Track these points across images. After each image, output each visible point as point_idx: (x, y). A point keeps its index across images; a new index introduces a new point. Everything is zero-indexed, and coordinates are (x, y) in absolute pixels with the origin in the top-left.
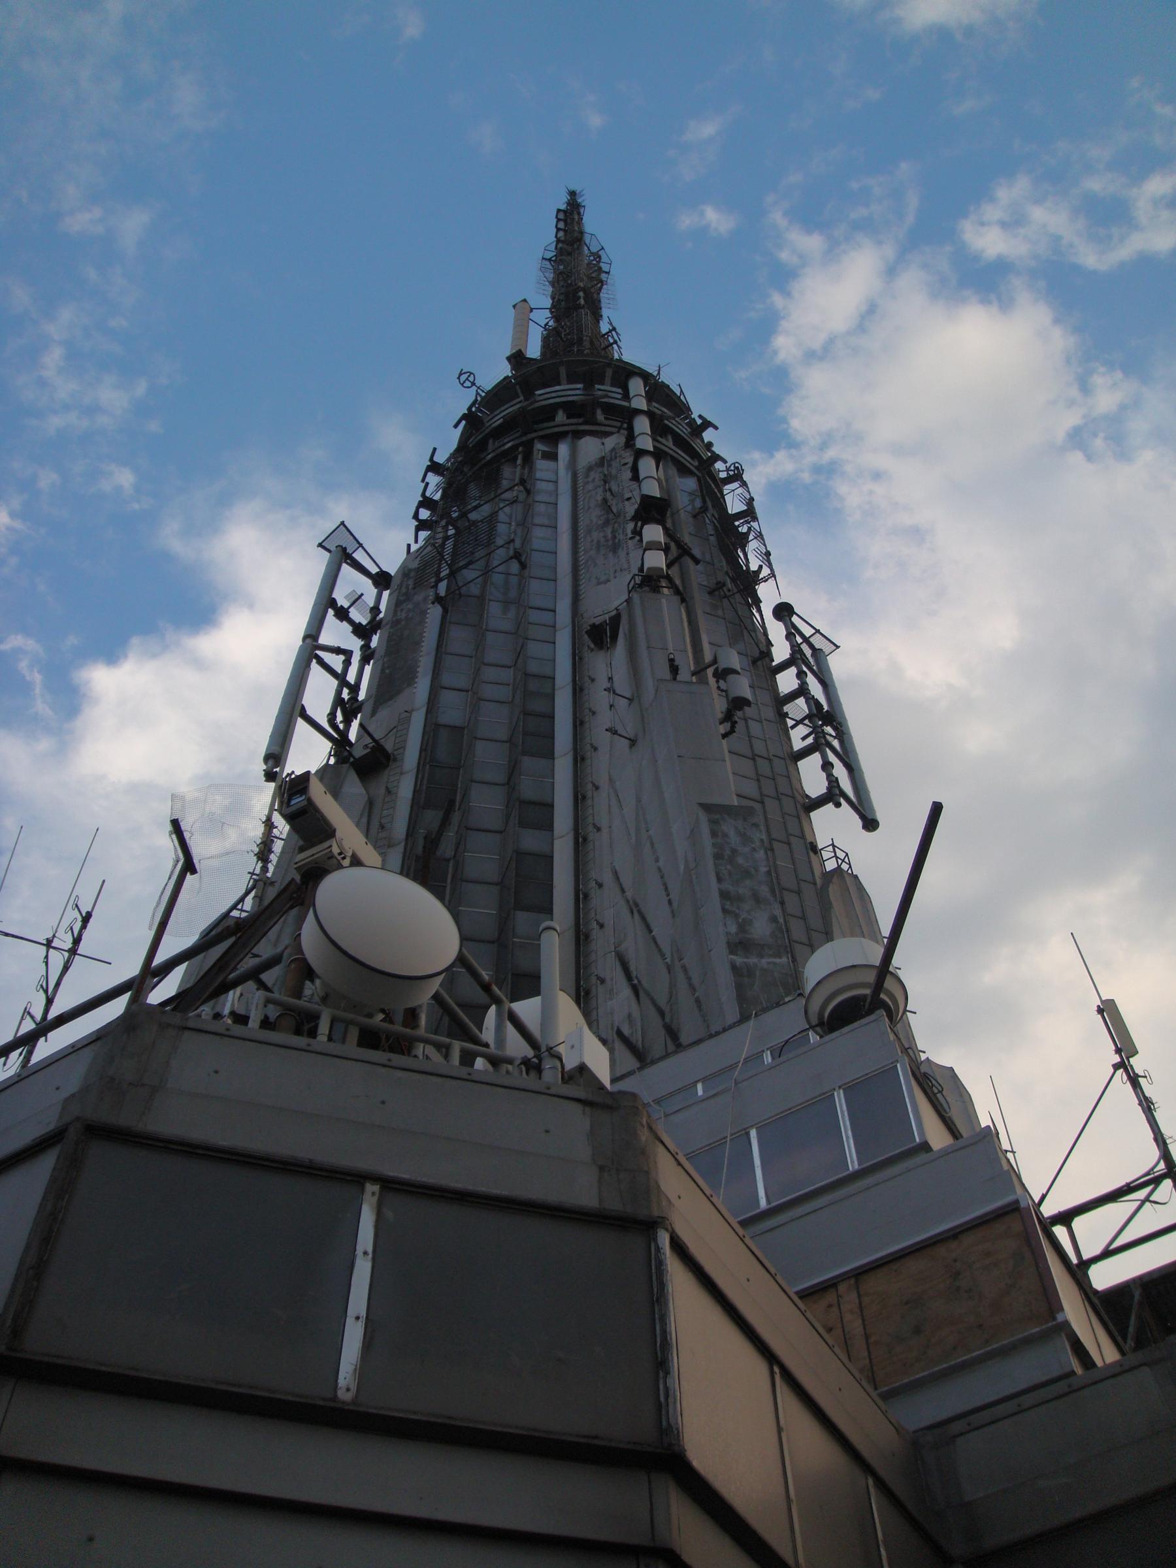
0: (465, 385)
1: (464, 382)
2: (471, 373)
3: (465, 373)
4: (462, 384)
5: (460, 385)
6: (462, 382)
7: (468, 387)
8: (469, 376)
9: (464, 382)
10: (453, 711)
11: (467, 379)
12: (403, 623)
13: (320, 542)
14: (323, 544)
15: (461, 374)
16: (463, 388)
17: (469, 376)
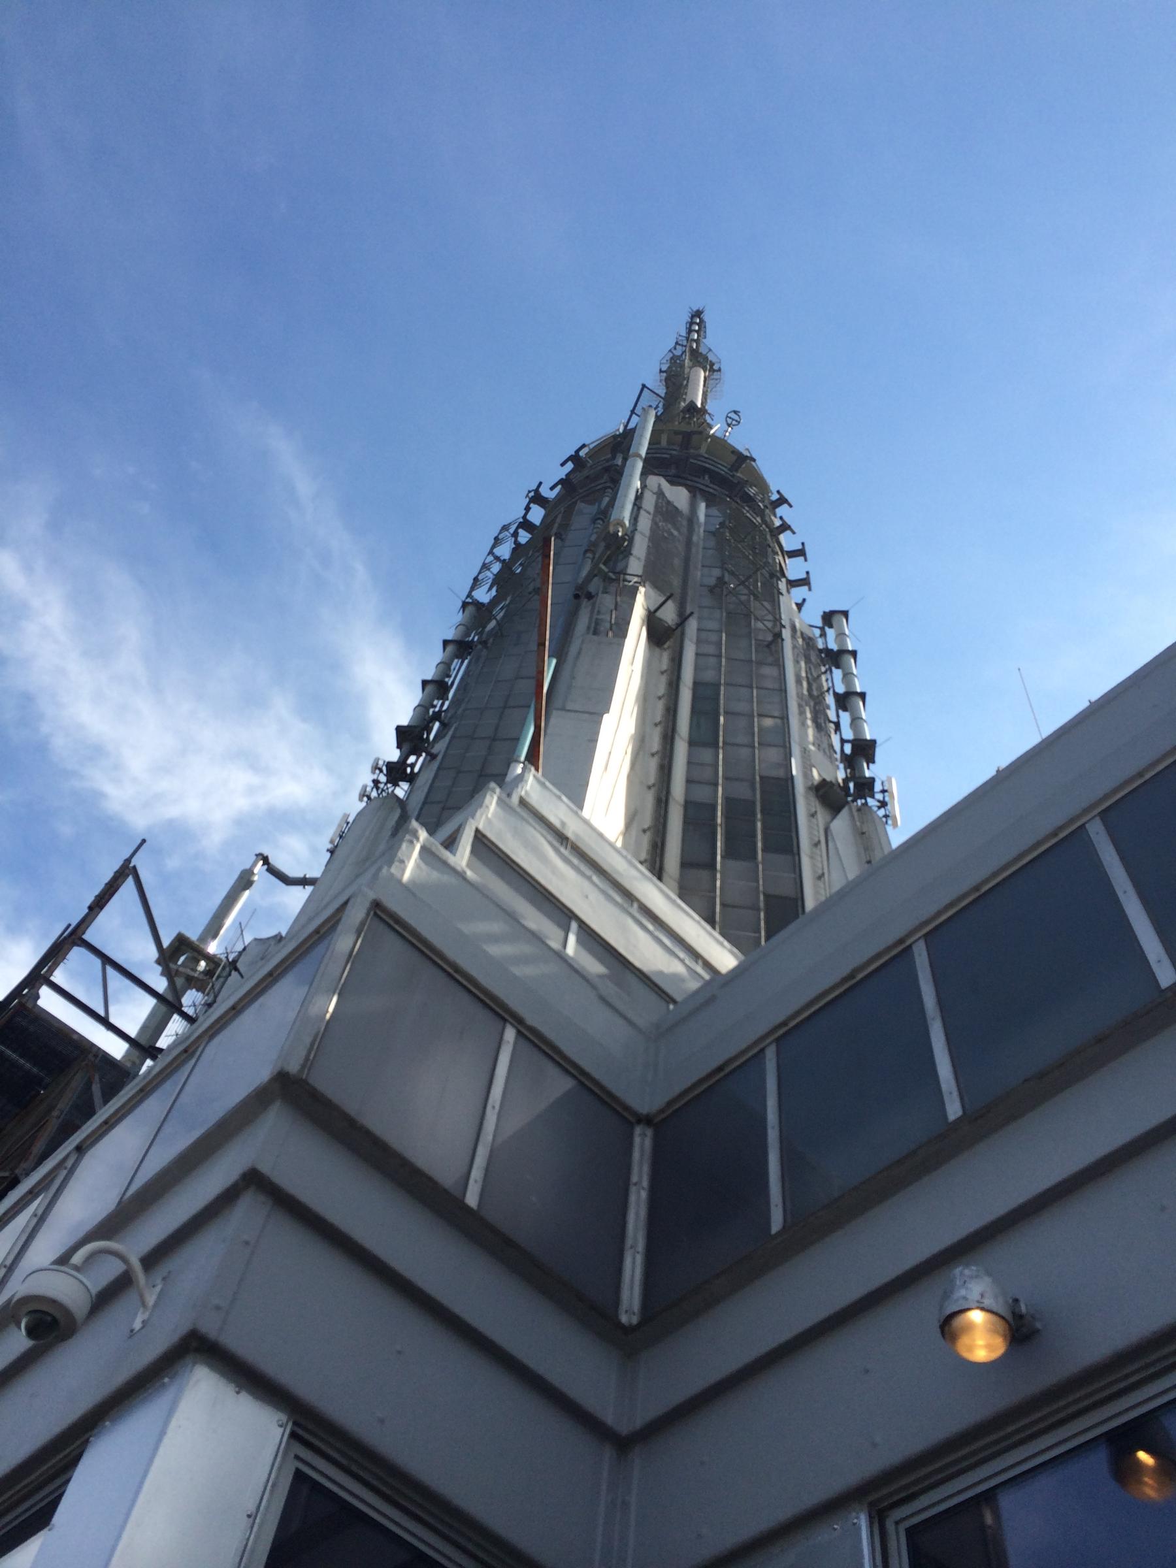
0: (728, 419)
1: (730, 418)
2: (739, 422)
3: (738, 415)
4: (727, 417)
5: (726, 414)
6: (729, 415)
7: (726, 421)
8: (736, 421)
9: (730, 418)
10: (709, 676)
11: (733, 420)
12: (660, 532)
13: (647, 385)
14: (645, 389)
15: (735, 412)
16: (724, 420)
17: (736, 421)
